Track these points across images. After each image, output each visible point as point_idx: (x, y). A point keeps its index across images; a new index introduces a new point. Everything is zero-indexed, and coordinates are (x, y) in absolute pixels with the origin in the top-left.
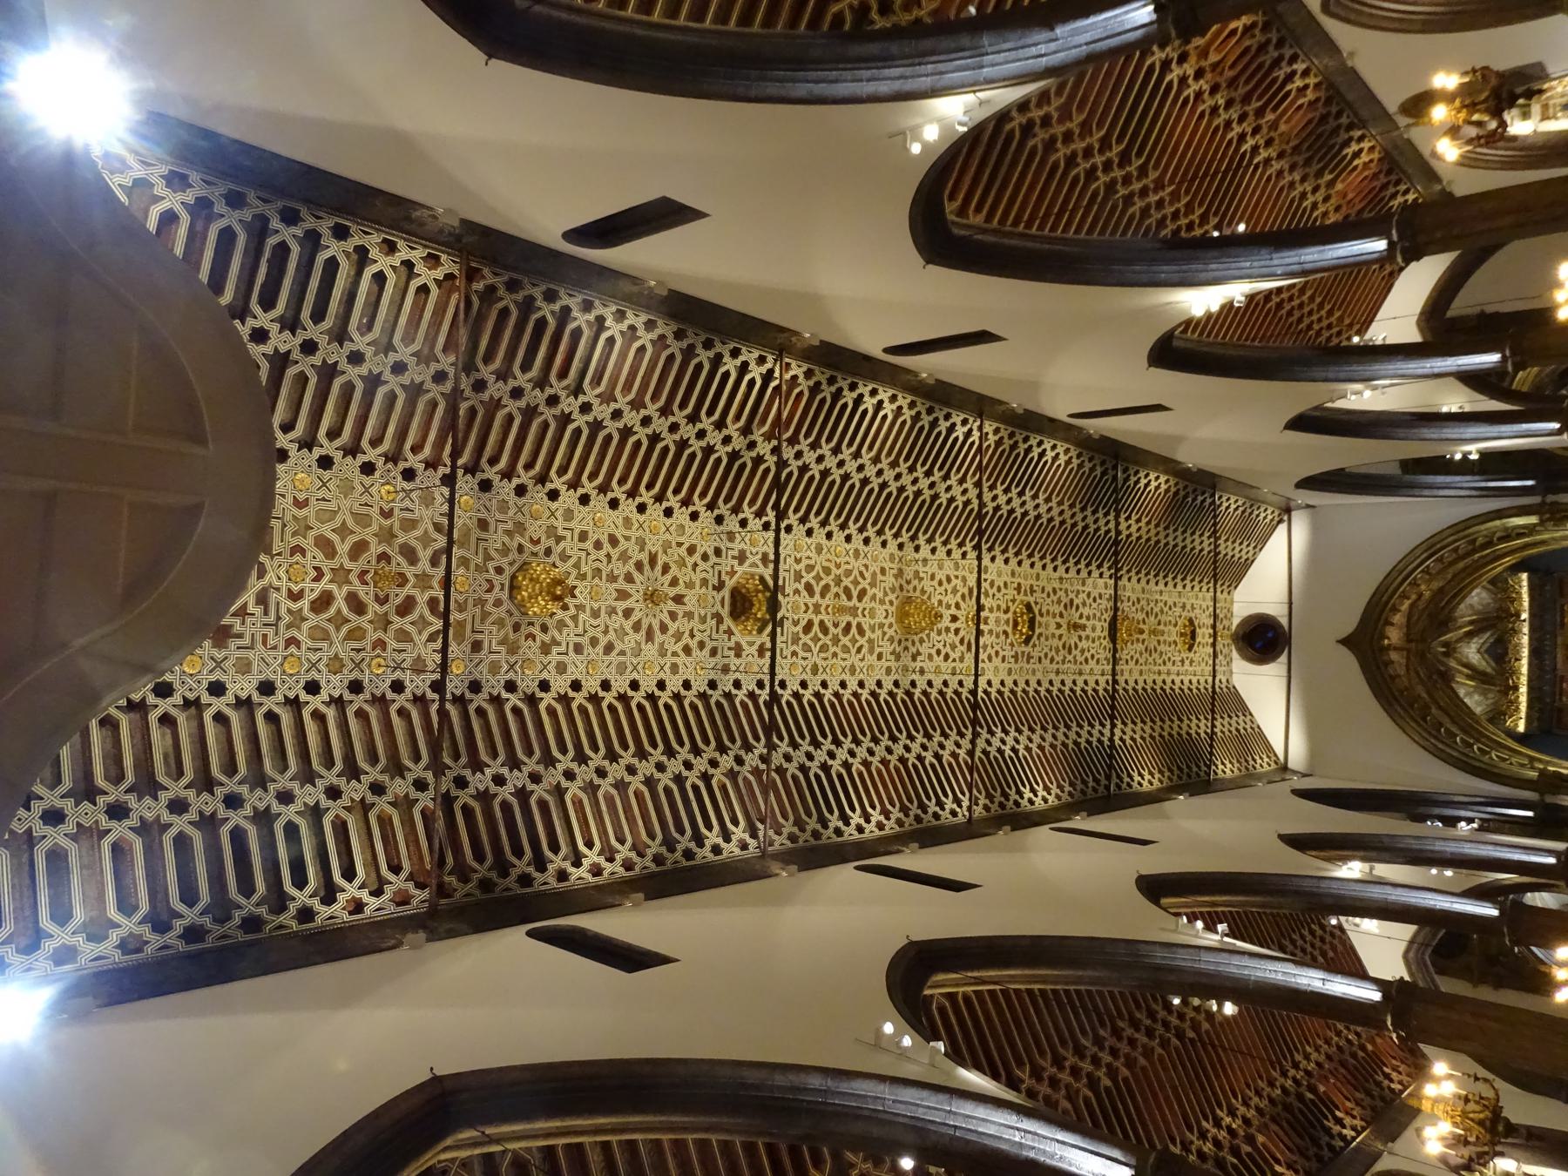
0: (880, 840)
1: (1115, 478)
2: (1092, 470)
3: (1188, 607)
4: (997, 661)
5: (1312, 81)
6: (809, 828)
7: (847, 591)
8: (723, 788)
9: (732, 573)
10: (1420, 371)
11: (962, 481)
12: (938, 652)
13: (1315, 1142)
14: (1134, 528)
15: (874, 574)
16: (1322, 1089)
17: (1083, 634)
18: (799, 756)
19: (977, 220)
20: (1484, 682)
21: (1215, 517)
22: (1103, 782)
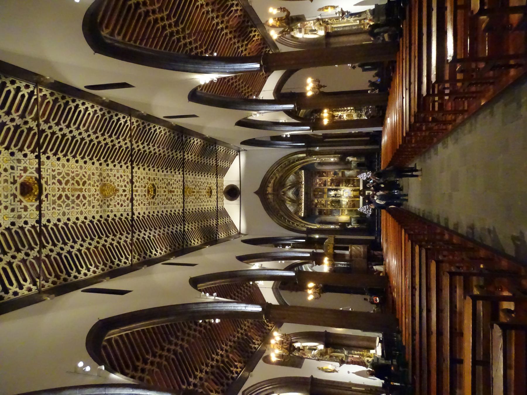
0: (95, 277)
1: (182, 140)
2: (174, 137)
4: (142, 205)
5: (239, 8)
6: (62, 278)
7: (78, 182)
8: (19, 267)
9: (21, 177)
11: (124, 140)
12: (118, 204)
13: (247, 352)
14: (190, 157)
15: (89, 175)
16: (249, 334)
17: (174, 194)
18: (57, 249)
19: (120, 38)
21: (216, 154)
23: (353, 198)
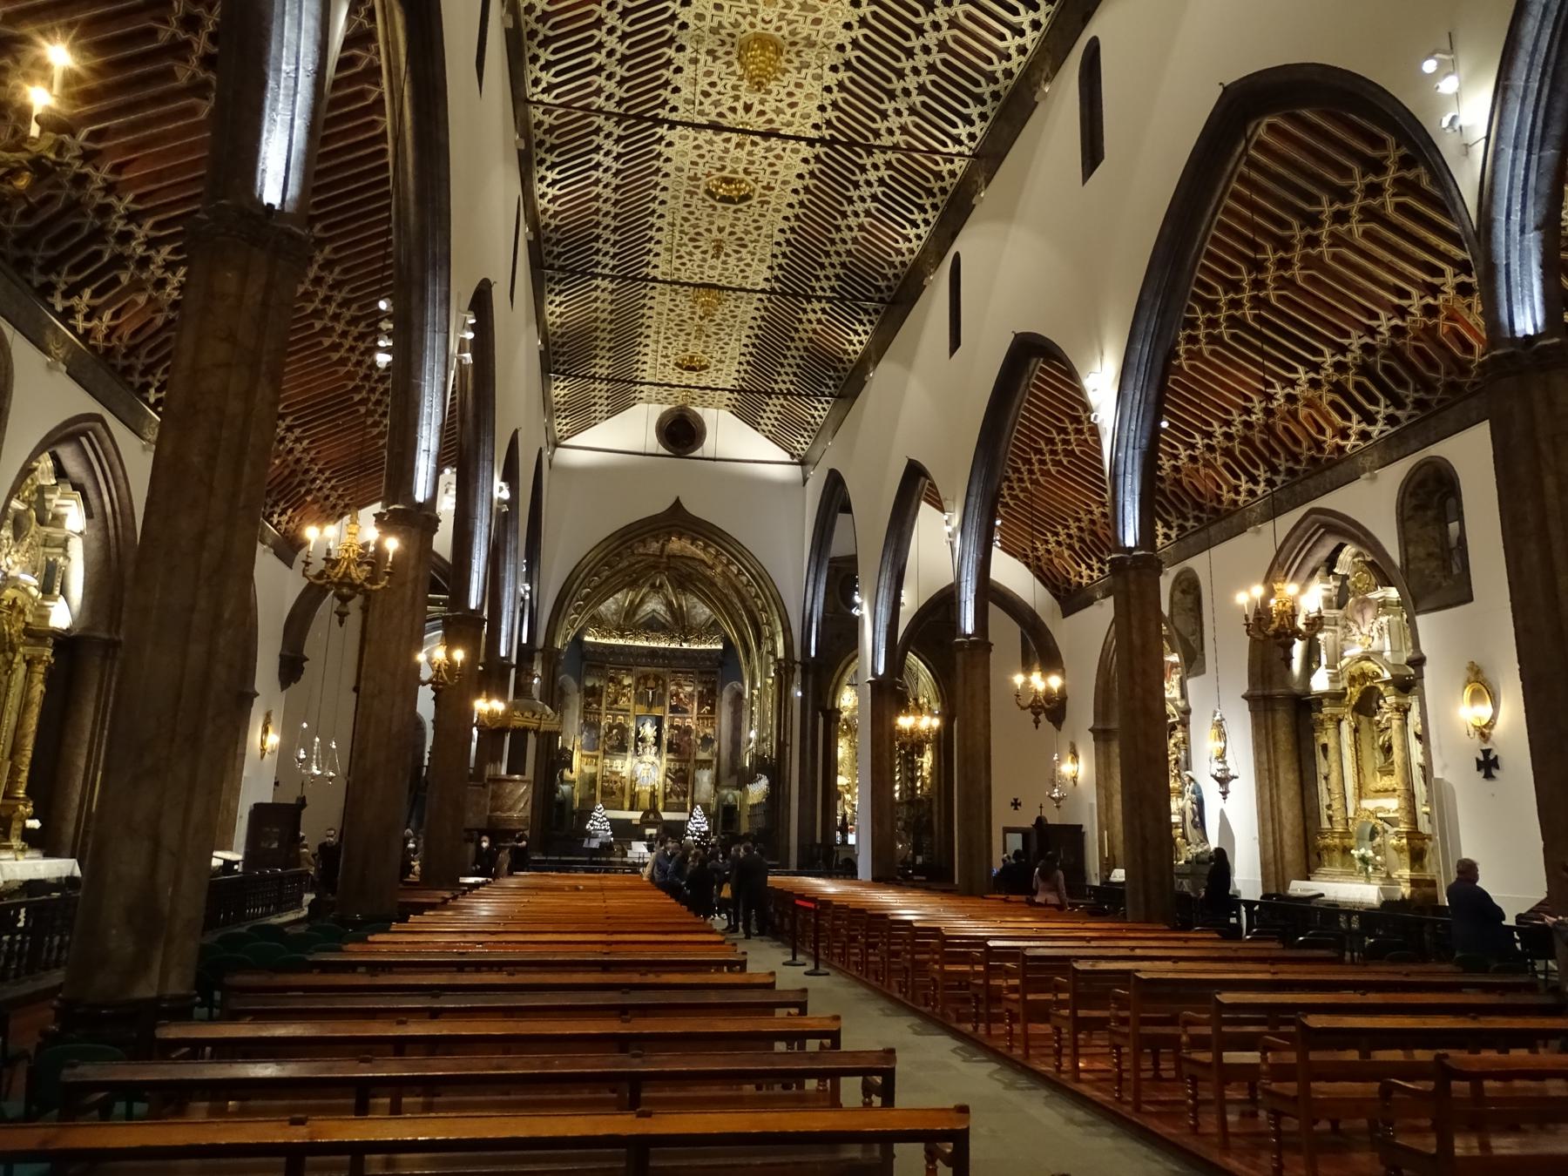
1: (871, 300)
2: (885, 277)
4: (693, 155)
11: (904, 130)
12: (713, 84)
14: (812, 316)
20: (627, 614)
21: (807, 395)
22: (557, 263)
23: (632, 790)
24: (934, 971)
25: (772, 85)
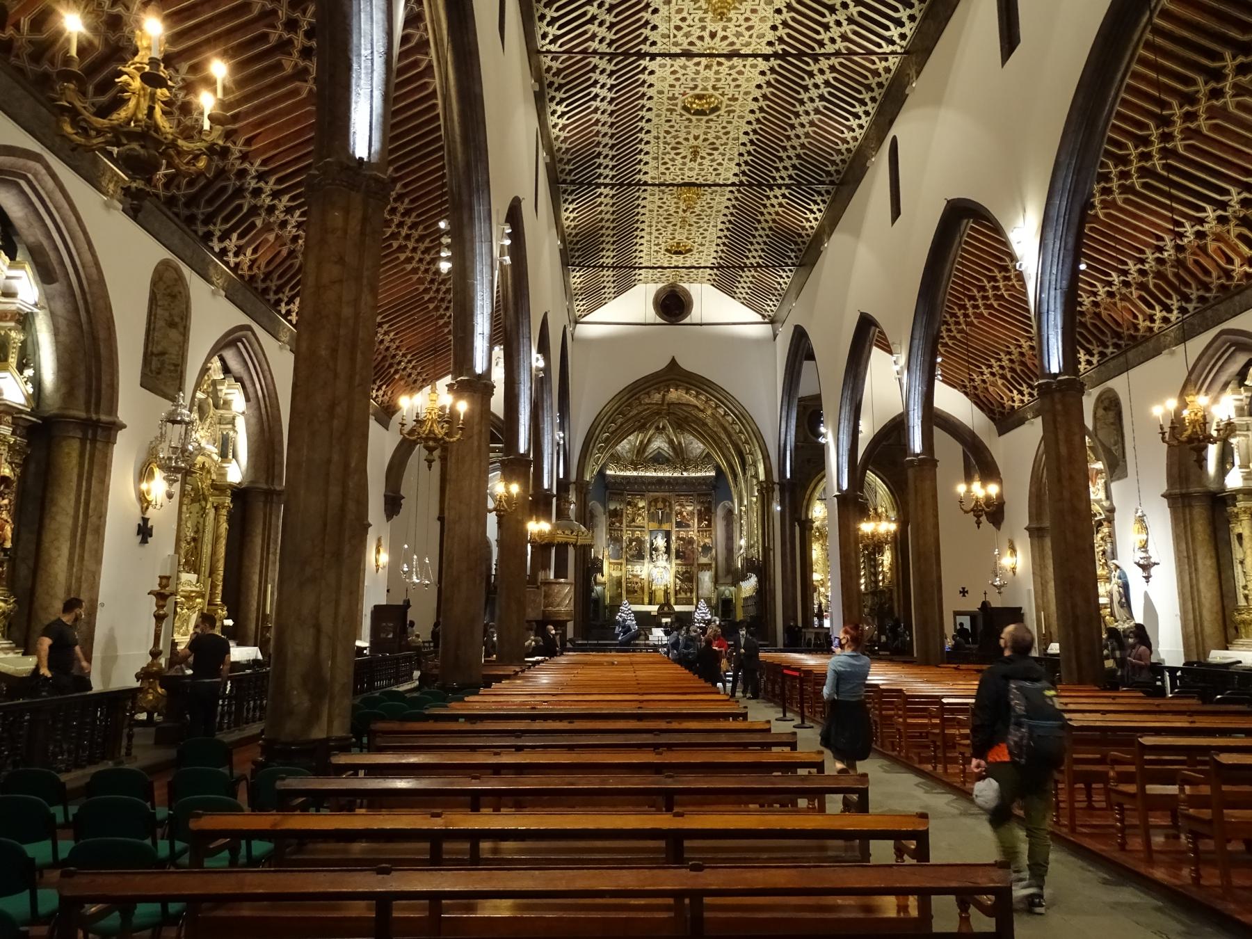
2: (834, 163)
3: (701, 248)
10: (912, 403)
11: (844, 37)
12: (683, 19)
14: (774, 201)
22: (569, 179)
24: (899, 723)
25: (732, 14)
